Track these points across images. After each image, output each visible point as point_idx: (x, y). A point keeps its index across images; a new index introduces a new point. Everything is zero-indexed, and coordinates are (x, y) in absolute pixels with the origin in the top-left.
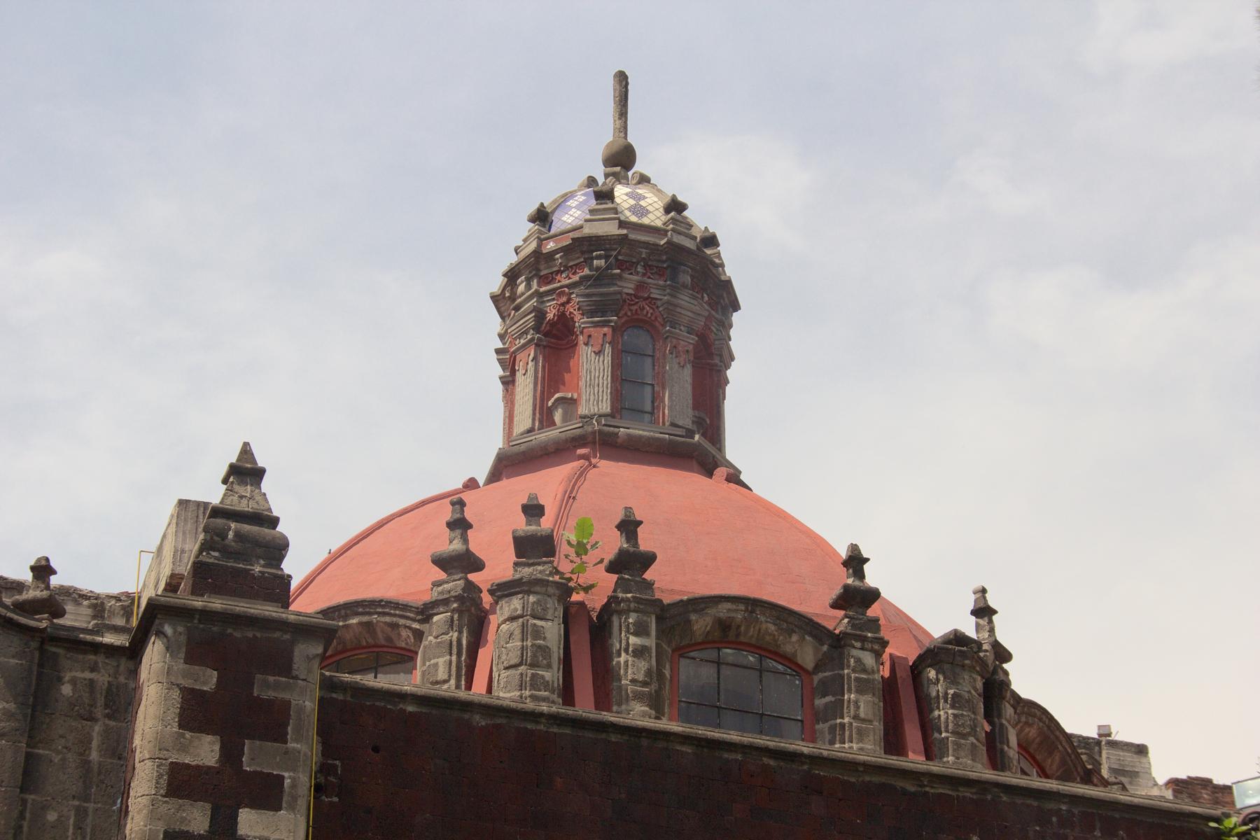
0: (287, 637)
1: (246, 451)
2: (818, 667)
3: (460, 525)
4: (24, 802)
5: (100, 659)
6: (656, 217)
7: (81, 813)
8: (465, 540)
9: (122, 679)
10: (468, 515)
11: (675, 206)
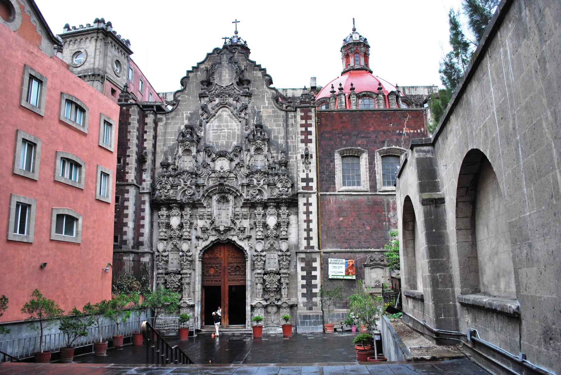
3: (333, 87)
6: (358, 39)
10: (334, 86)
11: (360, 36)
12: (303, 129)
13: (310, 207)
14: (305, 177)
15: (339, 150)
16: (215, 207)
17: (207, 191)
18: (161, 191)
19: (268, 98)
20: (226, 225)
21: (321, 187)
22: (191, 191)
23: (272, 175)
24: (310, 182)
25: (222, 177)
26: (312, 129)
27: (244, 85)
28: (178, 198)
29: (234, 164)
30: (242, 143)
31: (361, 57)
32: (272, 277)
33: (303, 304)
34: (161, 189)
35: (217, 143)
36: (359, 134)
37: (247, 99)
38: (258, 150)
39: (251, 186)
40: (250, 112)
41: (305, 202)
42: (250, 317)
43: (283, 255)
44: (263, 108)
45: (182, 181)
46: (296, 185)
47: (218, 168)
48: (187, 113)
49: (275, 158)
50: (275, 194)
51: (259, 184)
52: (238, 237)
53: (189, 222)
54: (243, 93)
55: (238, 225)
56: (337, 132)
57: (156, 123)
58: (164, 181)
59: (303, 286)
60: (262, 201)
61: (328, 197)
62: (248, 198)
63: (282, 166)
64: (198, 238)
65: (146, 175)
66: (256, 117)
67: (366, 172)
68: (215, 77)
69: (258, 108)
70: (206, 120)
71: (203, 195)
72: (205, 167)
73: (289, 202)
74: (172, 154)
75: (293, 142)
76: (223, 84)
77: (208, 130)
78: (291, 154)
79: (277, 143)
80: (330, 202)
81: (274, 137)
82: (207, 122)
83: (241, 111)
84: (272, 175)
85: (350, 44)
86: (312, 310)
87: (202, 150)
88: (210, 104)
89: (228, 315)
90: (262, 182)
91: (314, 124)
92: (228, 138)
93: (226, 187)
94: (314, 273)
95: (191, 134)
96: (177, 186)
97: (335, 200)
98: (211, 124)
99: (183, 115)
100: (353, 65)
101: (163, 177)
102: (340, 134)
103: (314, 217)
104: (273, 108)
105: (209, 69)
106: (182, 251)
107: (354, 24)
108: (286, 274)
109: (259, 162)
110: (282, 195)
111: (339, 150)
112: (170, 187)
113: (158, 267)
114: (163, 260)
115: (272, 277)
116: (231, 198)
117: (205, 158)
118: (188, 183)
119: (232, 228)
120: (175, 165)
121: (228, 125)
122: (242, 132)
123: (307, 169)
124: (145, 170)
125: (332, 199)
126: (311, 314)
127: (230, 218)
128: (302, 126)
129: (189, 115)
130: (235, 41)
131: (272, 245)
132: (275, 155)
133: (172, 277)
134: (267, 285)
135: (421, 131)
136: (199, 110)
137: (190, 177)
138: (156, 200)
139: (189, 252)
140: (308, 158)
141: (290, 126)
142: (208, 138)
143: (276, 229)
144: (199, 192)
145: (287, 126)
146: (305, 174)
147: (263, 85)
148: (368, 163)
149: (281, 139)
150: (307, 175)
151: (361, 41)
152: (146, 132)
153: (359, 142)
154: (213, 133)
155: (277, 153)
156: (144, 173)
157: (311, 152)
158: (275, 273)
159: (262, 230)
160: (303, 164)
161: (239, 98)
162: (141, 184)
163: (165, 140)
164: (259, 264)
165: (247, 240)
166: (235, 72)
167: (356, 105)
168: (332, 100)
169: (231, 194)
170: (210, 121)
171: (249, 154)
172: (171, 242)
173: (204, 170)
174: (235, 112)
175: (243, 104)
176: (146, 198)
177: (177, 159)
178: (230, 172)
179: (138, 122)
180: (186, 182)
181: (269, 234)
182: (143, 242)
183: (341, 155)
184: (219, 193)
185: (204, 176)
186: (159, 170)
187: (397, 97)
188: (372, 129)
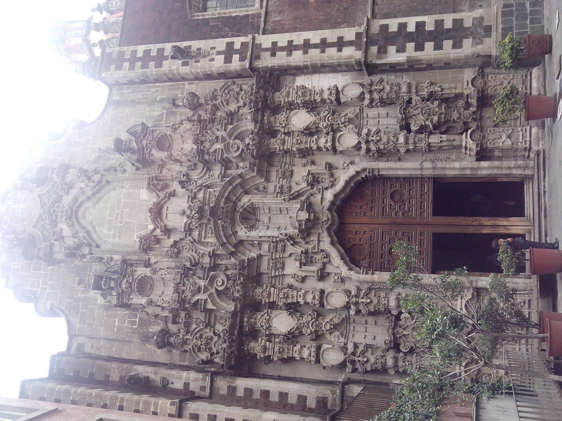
7: (140, 92)
13: (279, 45)
14: (223, 56)
16: (261, 234)
17: (223, 245)
18: (214, 350)
20: (297, 210)
22: (221, 278)
25: (201, 211)
28: (231, 307)
32: (416, 112)
33: (477, 44)
34: (210, 349)
39: (226, 155)
42: (505, 163)
43: (371, 92)
51: (223, 140)
52: (327, 189)
53: (286, 290)
55: (303, 186)
58: (195, 340)
59: (438, 47)
64: (323, 276)
65: (175, 381)
71: (232, 254)
72: (179, 252)
73: (264, 83)
78: (183, 93)
80: (279, 21)
82: (98, 246)
86: (491, 26)
87: (146, 257)
89: (501, 219)
90: (220, 134)
91: (132, 48)
93: (222, 205)
94: (411, 28)
101: (185, 342)
103: (298, 38)
106: (347, 307)
108: (409, 86)
112: (208, 330)
113: (379, 366)
114: (363, 353)
115: (416, 112)
116: (245, 200)
117: (163, 251)
118: (202, 283)
119: (308, 198)
120: (166, 317)
122: (127, 179)
124: (165, 382)
126: (500, 26)
127: (287, 205)
131: (350, 121)
132: (178, 120)
133: (405, 333)
134: (432, 122)
138: (229, 358)
139: (350, 292)
140: (189, 52)
143: (319, 114)
149: (154, 110)
155: (173, 113)
156: (171, 386)
158: (407, 107)
159: (316, 137)
160: (198, 61)
162: (193, 393)
164: (384, 140)
165: (334, 171)
169: (239, 199)
171: (168, 167)
172: (328, 336)
173: (185, 254)
175: (77, 176)
176: (222, 384)
178: (194, 198)
180: (199, 288)
181: (325, 124)
182: (318, 397)
184: (233, 223)
185: (196, 255)
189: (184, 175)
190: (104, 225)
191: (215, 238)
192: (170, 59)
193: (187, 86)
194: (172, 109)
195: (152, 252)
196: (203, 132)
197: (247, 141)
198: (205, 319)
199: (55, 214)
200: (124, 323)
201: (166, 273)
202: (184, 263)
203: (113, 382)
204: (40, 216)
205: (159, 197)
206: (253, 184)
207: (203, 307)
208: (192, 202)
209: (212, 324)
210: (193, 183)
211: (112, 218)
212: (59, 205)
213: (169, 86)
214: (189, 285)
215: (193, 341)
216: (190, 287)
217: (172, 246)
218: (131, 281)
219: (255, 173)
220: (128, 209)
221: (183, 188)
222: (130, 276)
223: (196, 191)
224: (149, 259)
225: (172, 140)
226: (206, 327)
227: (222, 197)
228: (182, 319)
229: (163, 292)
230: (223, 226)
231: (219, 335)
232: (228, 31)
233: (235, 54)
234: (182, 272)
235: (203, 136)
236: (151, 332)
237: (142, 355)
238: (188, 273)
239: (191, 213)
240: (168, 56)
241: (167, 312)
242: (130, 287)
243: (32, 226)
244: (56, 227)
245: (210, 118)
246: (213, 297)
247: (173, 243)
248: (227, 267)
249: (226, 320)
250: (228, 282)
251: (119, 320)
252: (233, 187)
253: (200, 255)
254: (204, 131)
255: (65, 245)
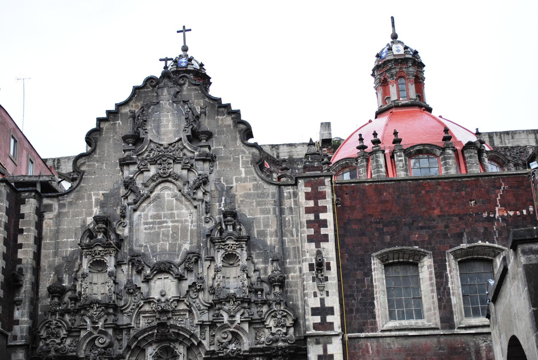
0: (323, 178)
1: (311, 140)
2: (441, 155)
3: (361, 139)
4: (281, 217)
5: (290, 187)
6: (402, 52)
8: (363, 142)
9: (295, 190)
10: (363, 137)
11: (406, 48)
12: (312, 217)
14: (319, 306)
15: (379, 253)
17: (135, 337)
18: (48, 342)
19: (245, 163)
21: (349, 325)
22: (106, 340)
23: (256, 303)
24: (327, 314)
25: (164, 312)
26: (328, 216)
27: (200, 141)
29: (185, 285)
30: (199, 247)
31: (410, 84)
34: (49, 338)
35: (153, 248)
36: (413, 221)
37: (207, 165)
38: (230, 258)
40: (213, 188)
41: (321, 353)
44: (237, 181)
45: (88, 321)
46: (301, 322)
47: (155, 295)
48: (98, 195)
49: (262, 272)
50: (263, 339)
51: (232, 322)
54: (200, 155)
56: (373, 220)
57: (40, 213)
58: (54, 322)
60: (239, 354)
61: (362, 341)
62: (212, 348)
63: (274, 286)
65: (20, 311)
66: (223, 198)
67: (432, 291)
68: (149, 128)
69: (226, 181)
70: (133, 206)
71: (129, 347)
72: (131, 294)
73: (290, 354)
74: (69, 271)
75: (292, 241)
76: (163, 140)
77: (138, 225)
78: (291, 263)
79: (265, 244)
80: (368, 352)
81: (259, 233)
82: (135, 210)
83: (198, 188)
84: (257, 304)
85: (389, 61)
87: (126, 261)
88: (141, 176)
90: (238, 318)
91: (330, 206)
92: (173, 237)
95: (106, 233)
96: (80, 332)
97: (377, 346)
98: (143, 213)
99: (90, 197)
100: (396, 98)
101: (54, 313)
102: (379, 223)
104: (255, 180)
105: (137, 115)
107: (393, 26)
109: (232, 280)
110: (277, 341)
111: (379, 253)
112: (65, 332)
117: (132, 276)
118: (100, 324)
120: (75, 290)
121: (174, 214)
122: (199, 226)
123: (322, 290)
124: (19, 303)
125: (371, 345)
128: (308, 210)
129: (102, 198)
130: (184, 64)
132: (260, 266)
135: (528, 211)
136: (119, 188)
137: (103, 313)
140: (321, 270)
141: (287, 212)
142: (137, 239)
144: (120, 340)
145: (282, 212)
146: (318, 299)
147: (236, 139)
148: (433, 275)
149: (271, 236)
150: (322, 301)
151: (407, 56)
152: (21, 231)
153: (415, 236)
154: (146, 229)
155: (265, 262)
156: (16, 308)
157: (327, 258)
160: (314, 281)
161: (192, 165)
162: (10, 329)
163: (57, 246)
166: (183, 118)
167: (406, 170)
168: (362, 161)
169: (181, 343)
170: (141, 208)
171: (213, 266)
174: (186, 190)
175: (199, 175)
177: (80, 280)
178: (179, 301)
179: (7, 214)
180: (97, 323)
183: (382, 261)
184: (158, 342)
185: (129, 310)
186: (46, 301)
187: (480, 152)
188: (437, 212)
189: (201, 286)
190: (156, 211)
191: (144, 327)
192: (317, 249)
193: (297, 266)
194: (271, 258)
195: (131, 266)
196: (239, 301)
197: (232, 347)
198: (74, 328)
199: (162, 162)
200: (71, 247)
201: (110, 287)
202: (124, 298)
203: (16, 253)
204: (162, 145)
205: (179, 266)
206: (196, 354)
207: (81, 327)
208: (174, 300)
209: (71, 334)
210: (196, 295)
211: (163, 217)
212: (171, 164)
213: (298, 247)
214: (98, 313)
215: (54, 320)
216: (96, 314)
217: (136, 285)
218: (101, 254)
219: (204, 356)
220: (171, 232)
221: (190, 287)
222: (106, 252)
223: (185, 301)
224: (125, 264)
225: (236, 266)
226: (67, 331)
227: (179, 330)
228: (72, 307)
229: (96, 284)
230: (153, 334)
231: (62, 342)
232: (358, 299)
233: (321, 318)
234: (112, 302)
235: (234, 302)
236: (63, 276)
237: (45, 270)
238: (111, 308)
239: (162, 302)
240: (320, 247)
241: (80, 290)
242: (96, 255)
243: (151, 139)
244: (151, 164)
245: (258, 301)
246: (90, 336)
247: (138, 286)
248: (122, 340)
249: (75, 346)
250: (102, 348)
251: (73, 241)
252: (189, 339)
253: (130, 314)
254: (240, 302)
255: (135, 178)
